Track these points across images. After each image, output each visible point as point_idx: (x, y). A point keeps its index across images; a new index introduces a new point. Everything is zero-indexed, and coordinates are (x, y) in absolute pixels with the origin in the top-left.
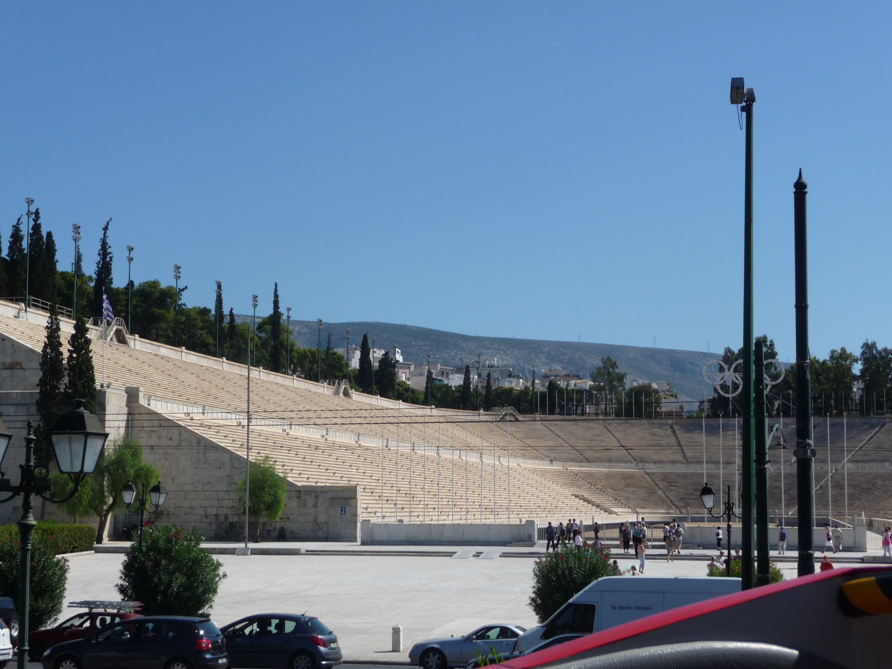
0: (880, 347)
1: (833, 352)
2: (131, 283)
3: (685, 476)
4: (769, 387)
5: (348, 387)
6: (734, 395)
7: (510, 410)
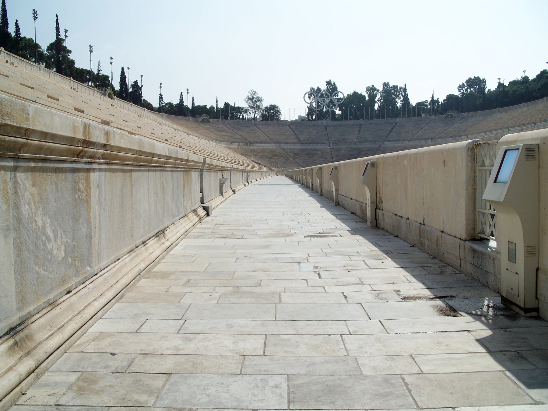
0: (391, 85)
1: (368, 87)
4: (337, 105)
6: (319, 109)
7: (205, 116)
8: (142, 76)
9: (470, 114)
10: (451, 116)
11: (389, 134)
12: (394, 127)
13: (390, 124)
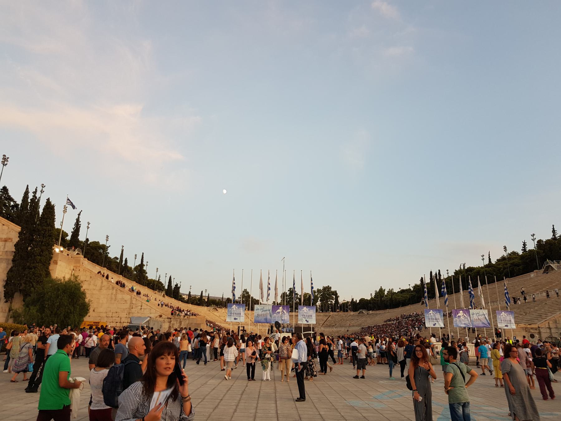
2: (87, 240)
5: (165, 294)
9: (373, 312)
10: (362, 312)
11: (324, 323)
12: (328, 318)
13: (326, 316)
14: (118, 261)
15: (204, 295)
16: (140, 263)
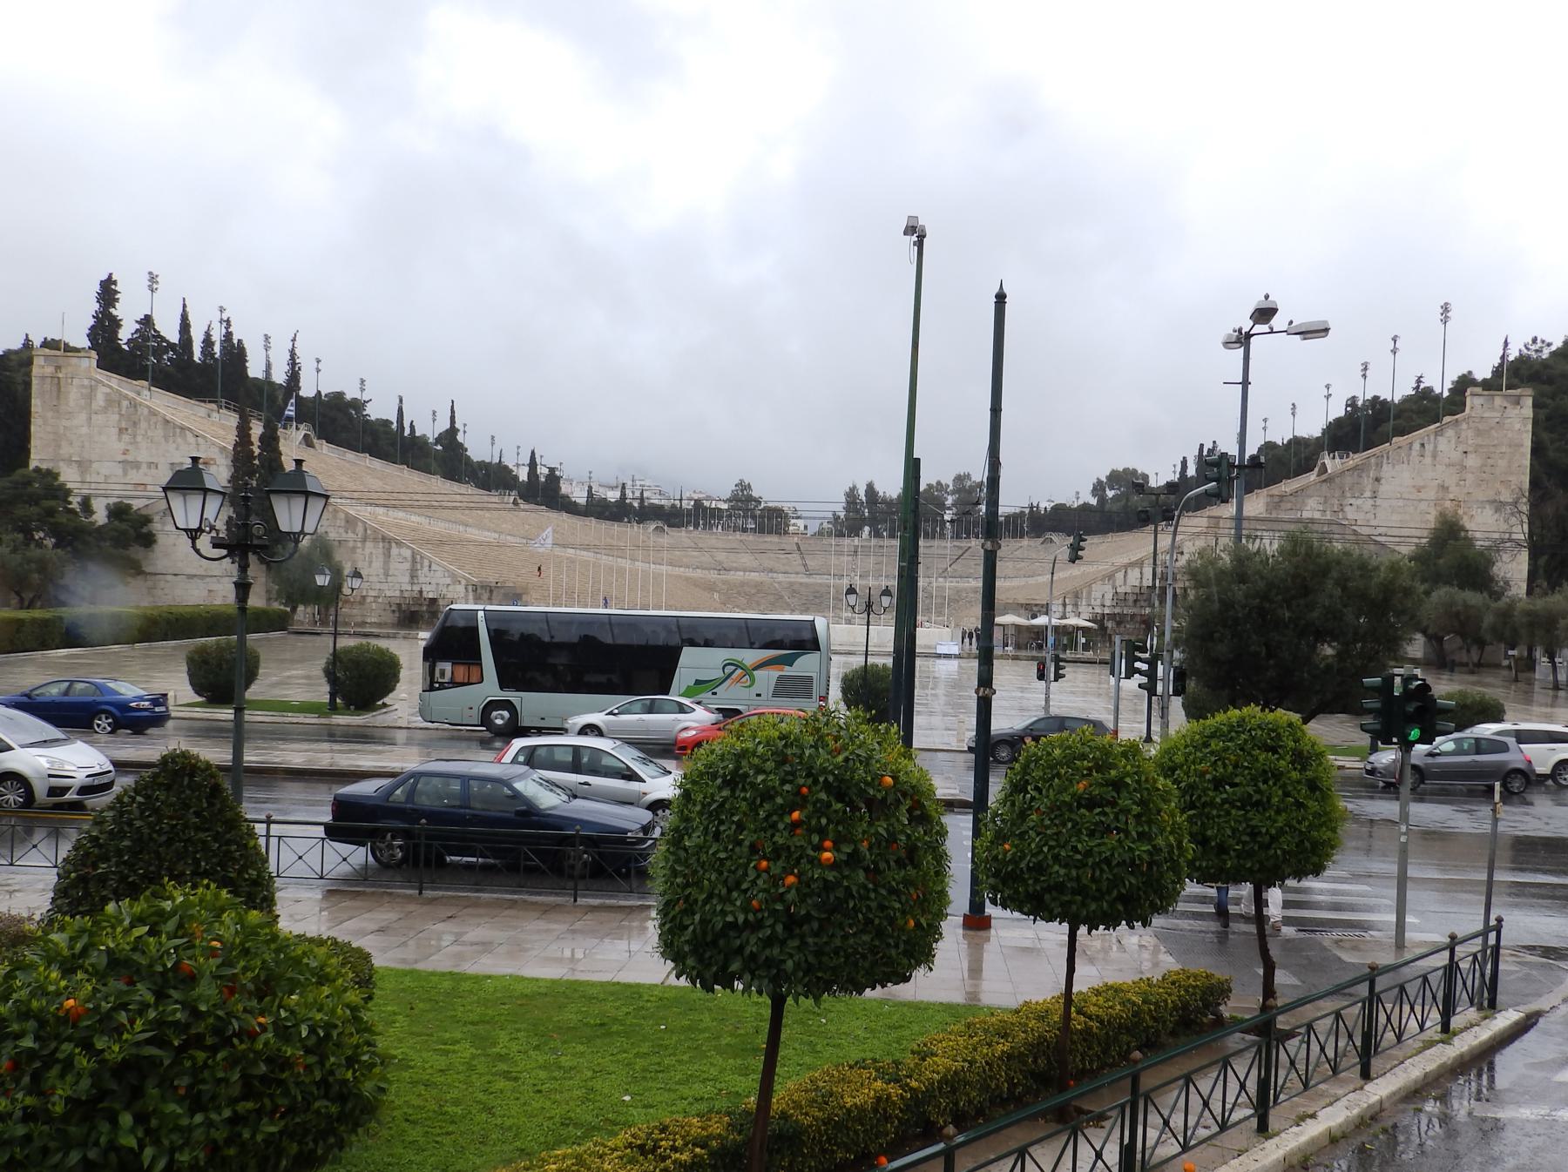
3: (807, 585)
8: (561, 464)
14: (394, 426)
15: (629, 494)
16: (448, 426)
